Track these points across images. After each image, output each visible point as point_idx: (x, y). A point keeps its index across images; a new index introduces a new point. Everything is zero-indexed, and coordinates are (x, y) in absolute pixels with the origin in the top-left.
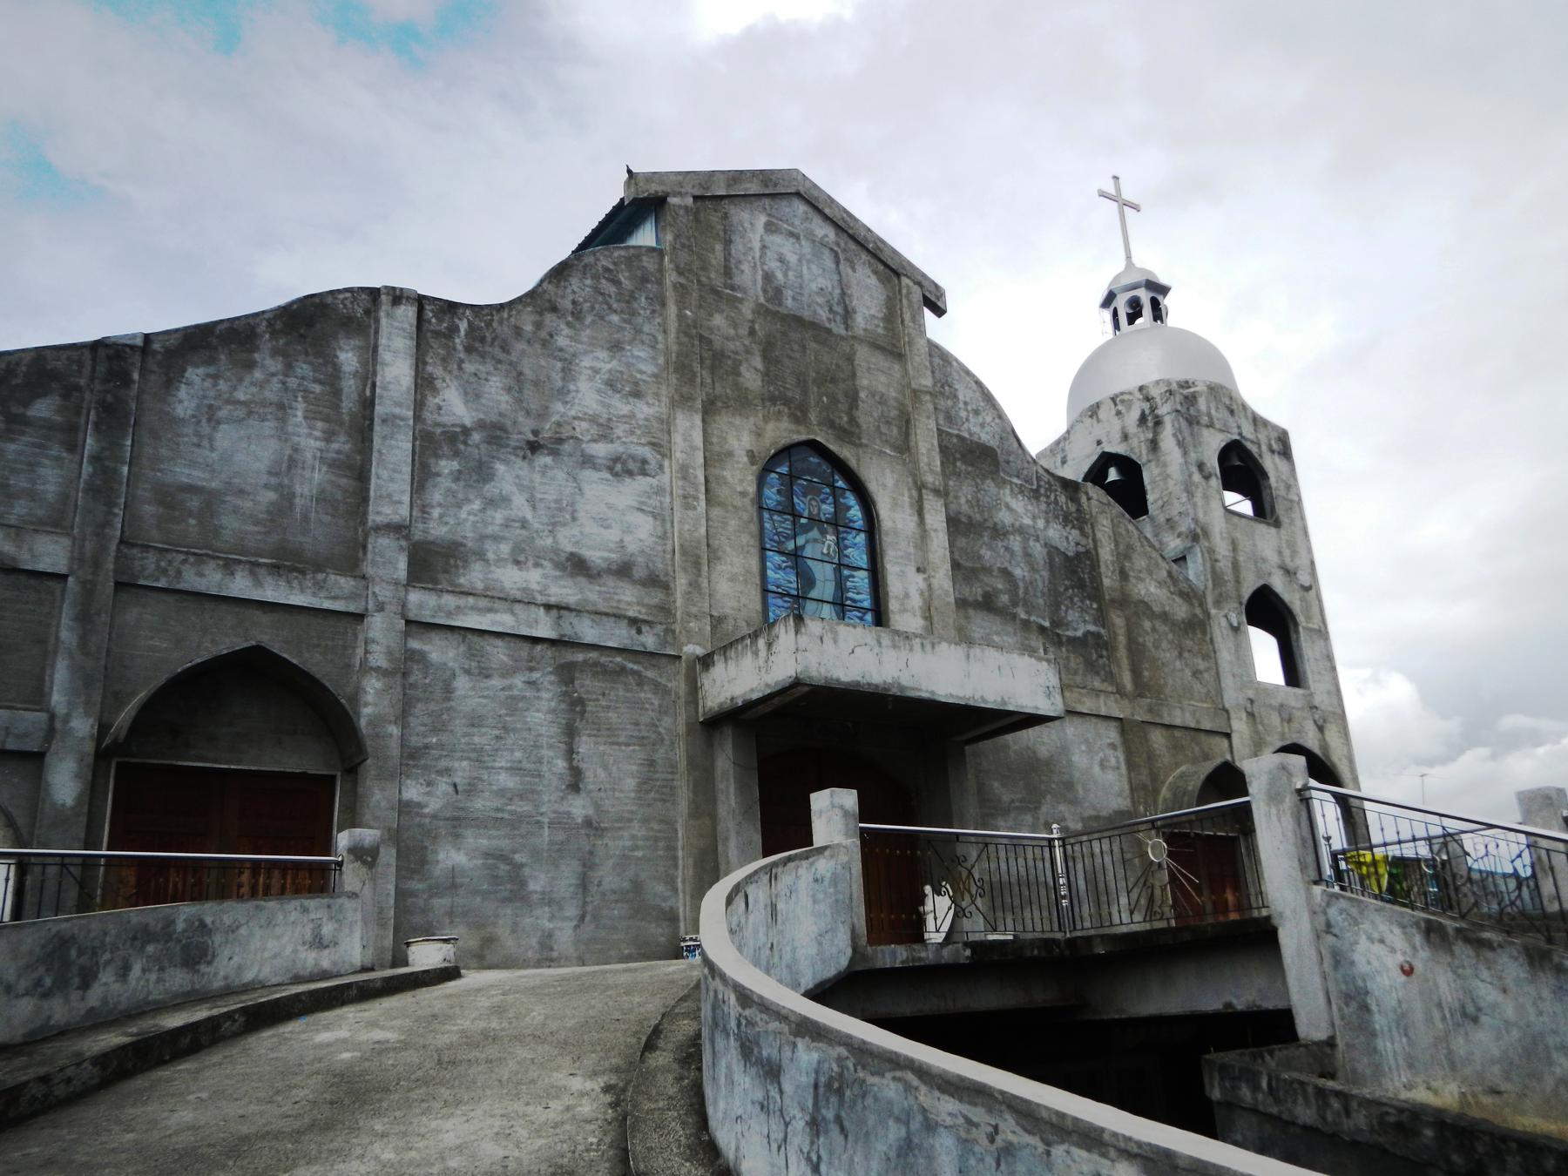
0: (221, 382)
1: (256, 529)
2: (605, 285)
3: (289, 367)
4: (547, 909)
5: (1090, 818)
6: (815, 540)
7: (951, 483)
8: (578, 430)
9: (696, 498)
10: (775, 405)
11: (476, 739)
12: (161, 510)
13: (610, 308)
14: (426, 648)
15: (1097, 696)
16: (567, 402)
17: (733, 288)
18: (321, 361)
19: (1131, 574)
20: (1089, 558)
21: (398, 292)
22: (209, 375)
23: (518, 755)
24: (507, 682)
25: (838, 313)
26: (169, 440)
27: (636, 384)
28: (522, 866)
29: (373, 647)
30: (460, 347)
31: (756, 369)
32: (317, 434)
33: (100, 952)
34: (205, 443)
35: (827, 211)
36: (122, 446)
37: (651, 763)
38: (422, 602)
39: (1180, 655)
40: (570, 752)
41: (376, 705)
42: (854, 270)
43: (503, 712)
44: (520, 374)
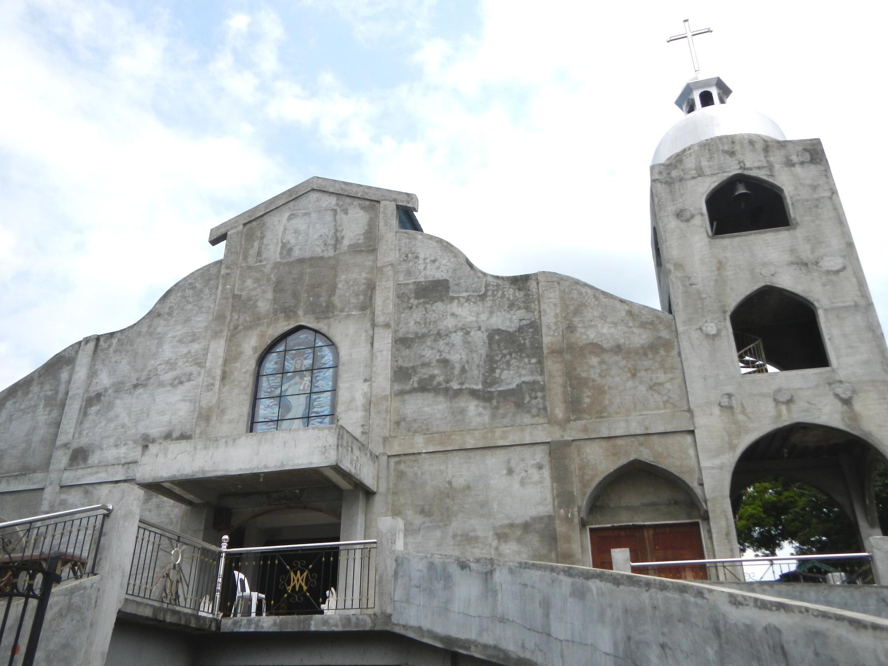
5: (502, 527)
6: (296, 384)
7: (403, 315)
8: (159, 370)
9: (213, 385)
10: (276, 315)
15: (522, 430)
16: (156, 359)
17: (261, 261)
19: (580, 325)
20: (531, 327)
25: (330, 244)
27: (194, 335)
31: (267, 300)
32: (46, 413)
35: (331, 190)
38: (69, 477)
39: (634, 375)
42: (346, 213)
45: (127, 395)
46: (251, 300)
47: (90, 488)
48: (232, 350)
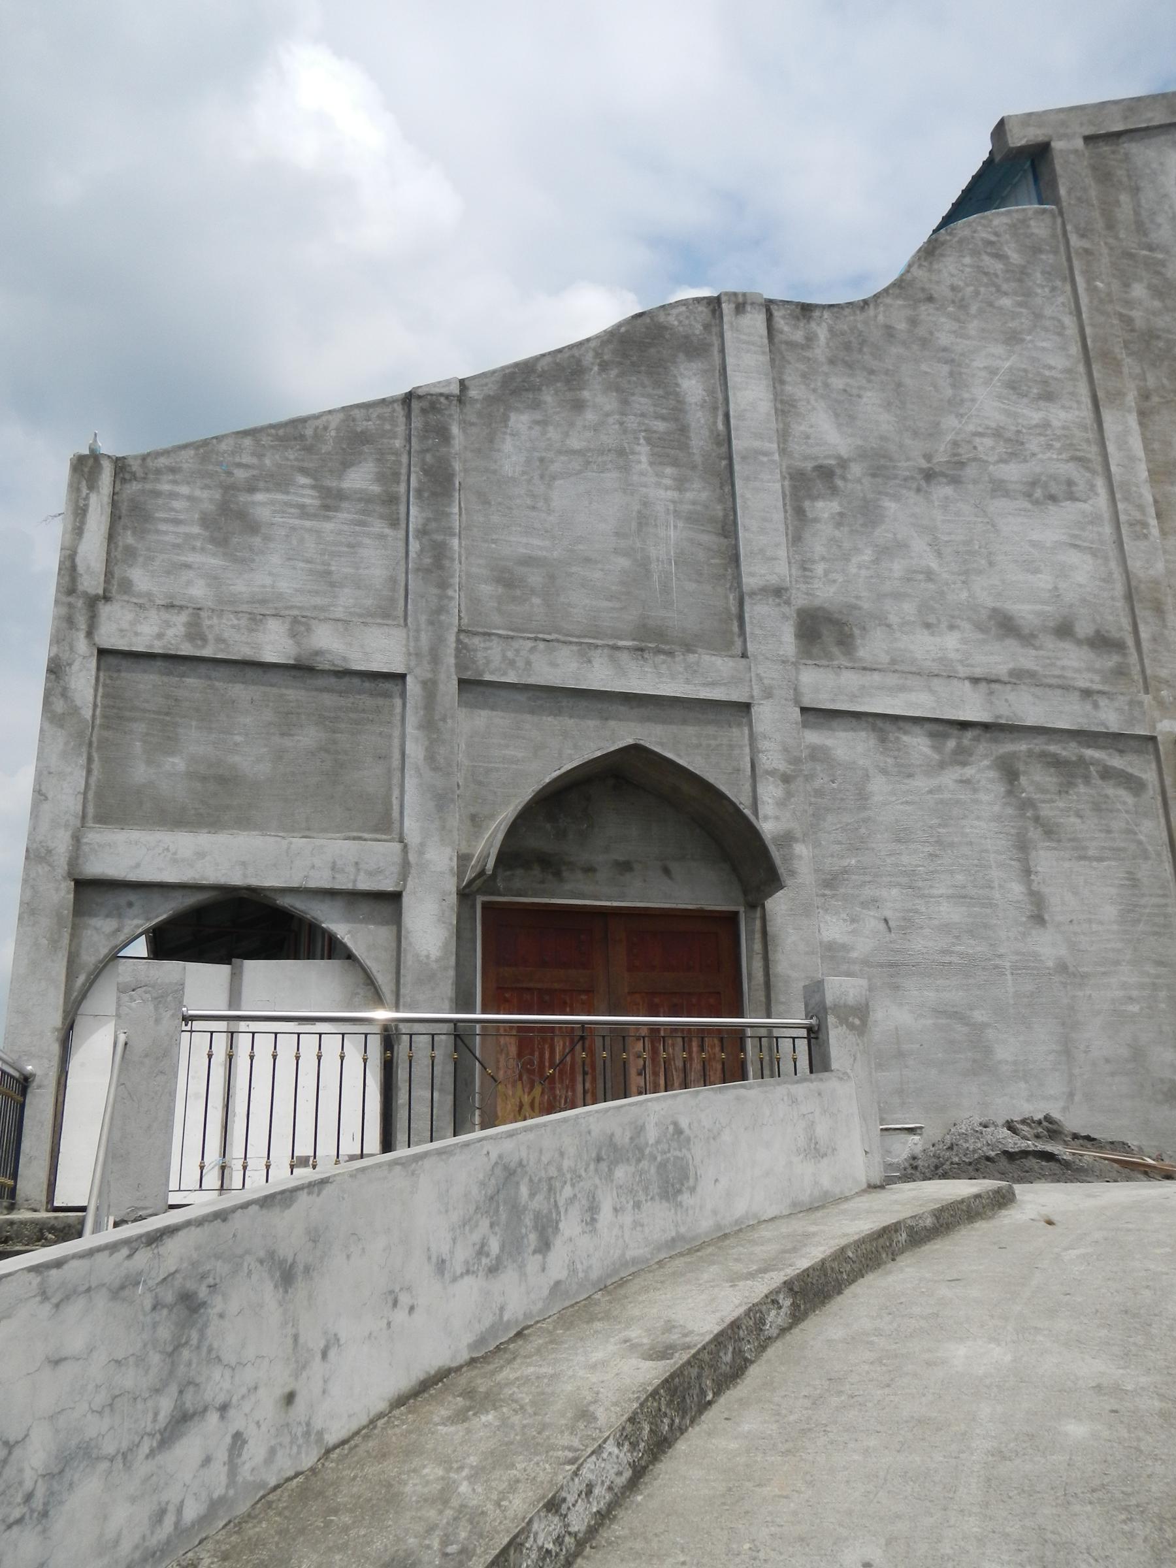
0: (551, 429)
1: (610, 604)
2: (987, 260)
3: (625, 402)
4: (1022, 1085)
8: (980, 448)
9: (1145, 525)
11: (905, 859)
12: (500, 590)
13: (999, 290)
14: (829, 742)
16: (962, 416)
17: (1151, 248)
18: (661, 392)
21: (741, 300)
22: (538, 423)
23: (960, 878)
24: (934, 782)
26: (500, 504)
27: (1045, 382)
28: (984, 1026)
29: (764, 745)
30: (822, 359)
32: (667, 482)
33: (558, 1184)
34: (540, 504)
36: (448, 515)
37: (1133, 882)
40: (1027, 872)
41: (777, 818)
43: (935, 821)
44: (899, 385)
45: (912, 494)
46: (1158, 337)
47: (888, 726)
48: (1153, 450)
